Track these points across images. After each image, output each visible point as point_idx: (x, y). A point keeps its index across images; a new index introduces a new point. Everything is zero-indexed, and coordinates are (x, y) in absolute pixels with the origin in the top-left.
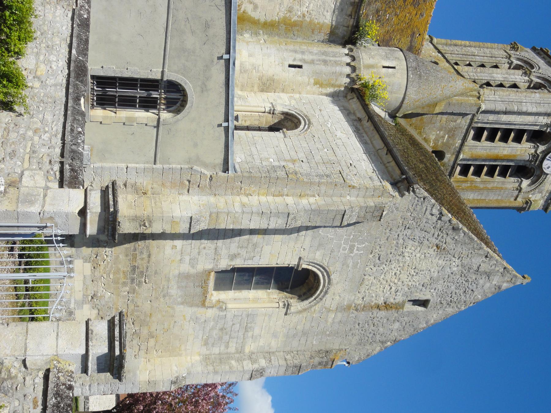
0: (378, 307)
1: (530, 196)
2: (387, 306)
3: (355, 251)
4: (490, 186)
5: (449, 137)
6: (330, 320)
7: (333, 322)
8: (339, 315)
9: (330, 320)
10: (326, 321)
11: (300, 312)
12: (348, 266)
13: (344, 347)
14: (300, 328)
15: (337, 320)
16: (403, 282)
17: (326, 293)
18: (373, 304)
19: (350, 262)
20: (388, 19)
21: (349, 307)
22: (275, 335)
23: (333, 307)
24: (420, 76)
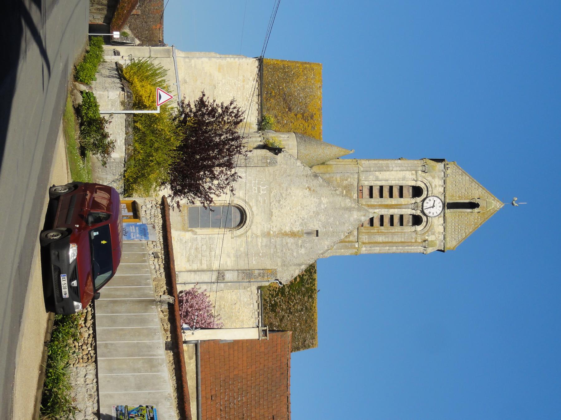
0: (285, 234)
1: (427, 238)
2: (293, 234)
3: (262, 192)
4: (393, 231)
5: (346, 192)
6: (259, 244)
7: (262, 246)
8: (264, 239)
9: (259, 244)
10: (257, 245)
11: (239, 236)
12: (260, 202)
13: (274, 268)
14: (242, 249)
15: (264, 244)
16: (297, 215)
17: (252, 222)
18: (283, 231)
19: (260, 199)
20: (286, 124)
21: (269, 233)
22: (229, 256)
23: (259, 233)
24: (305, 141)
